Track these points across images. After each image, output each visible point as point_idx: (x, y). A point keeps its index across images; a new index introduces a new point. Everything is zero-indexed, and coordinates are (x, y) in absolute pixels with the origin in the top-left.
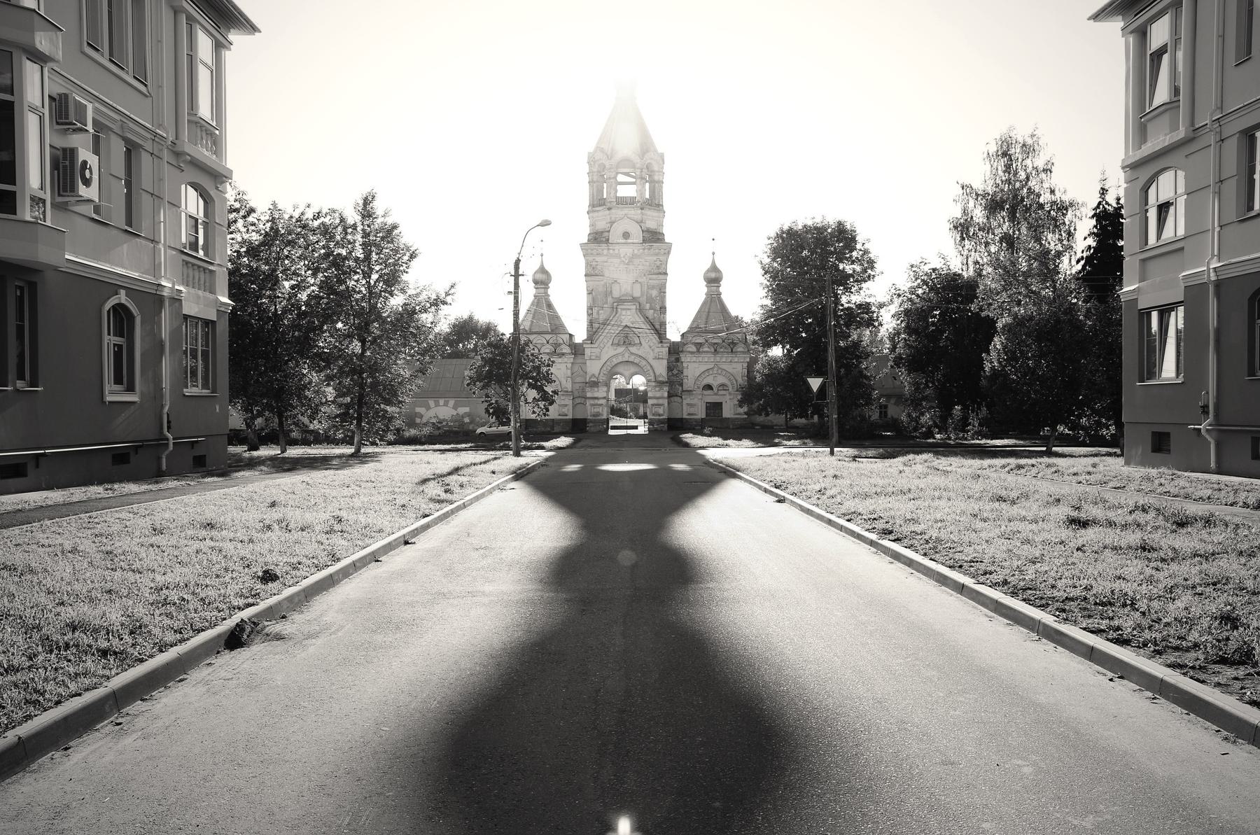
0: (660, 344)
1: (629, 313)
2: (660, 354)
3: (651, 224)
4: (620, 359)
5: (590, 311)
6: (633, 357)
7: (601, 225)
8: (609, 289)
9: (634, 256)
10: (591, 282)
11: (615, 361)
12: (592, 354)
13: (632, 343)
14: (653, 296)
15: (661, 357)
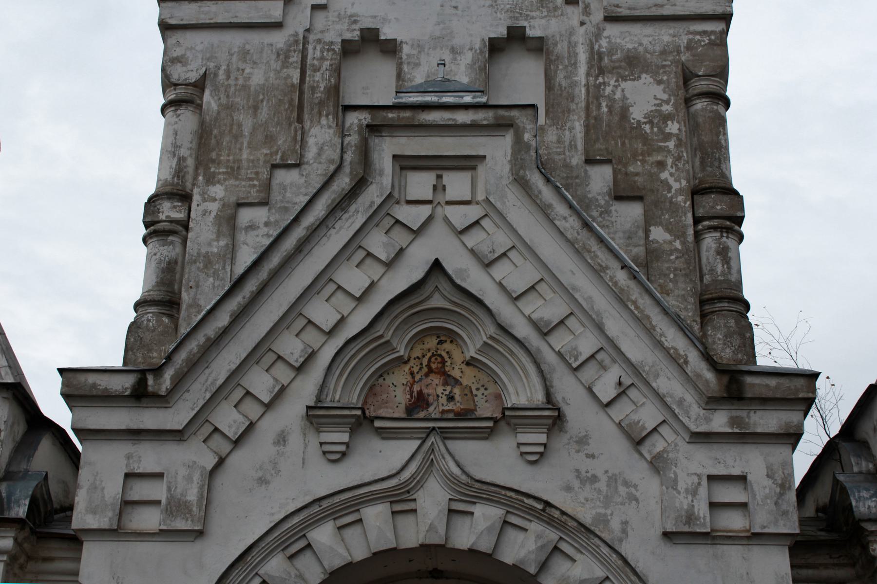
0: (719, 422)
2: (731, 494)
5: (169, 211)
8: (320, 79)
10: (199, 40)
12: (141, 490)
13: (486, 409)
14: (637, 114)
15: (734, 522)
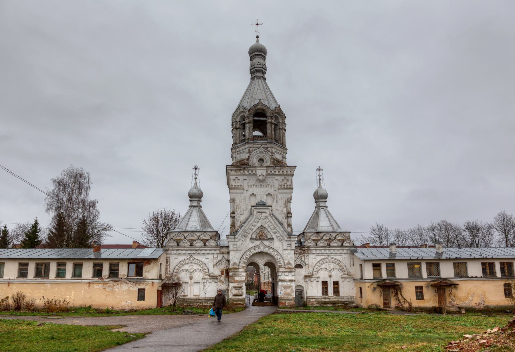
1: (263, 214)
3: (278, 157)
4: (258, 250)
6: (267, 249)
7: (244, 156)
9: (267, 176)
11: (253, 252)
